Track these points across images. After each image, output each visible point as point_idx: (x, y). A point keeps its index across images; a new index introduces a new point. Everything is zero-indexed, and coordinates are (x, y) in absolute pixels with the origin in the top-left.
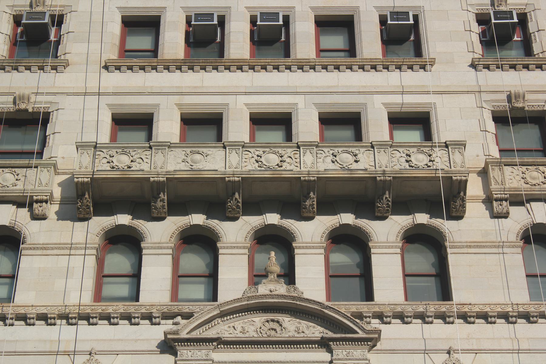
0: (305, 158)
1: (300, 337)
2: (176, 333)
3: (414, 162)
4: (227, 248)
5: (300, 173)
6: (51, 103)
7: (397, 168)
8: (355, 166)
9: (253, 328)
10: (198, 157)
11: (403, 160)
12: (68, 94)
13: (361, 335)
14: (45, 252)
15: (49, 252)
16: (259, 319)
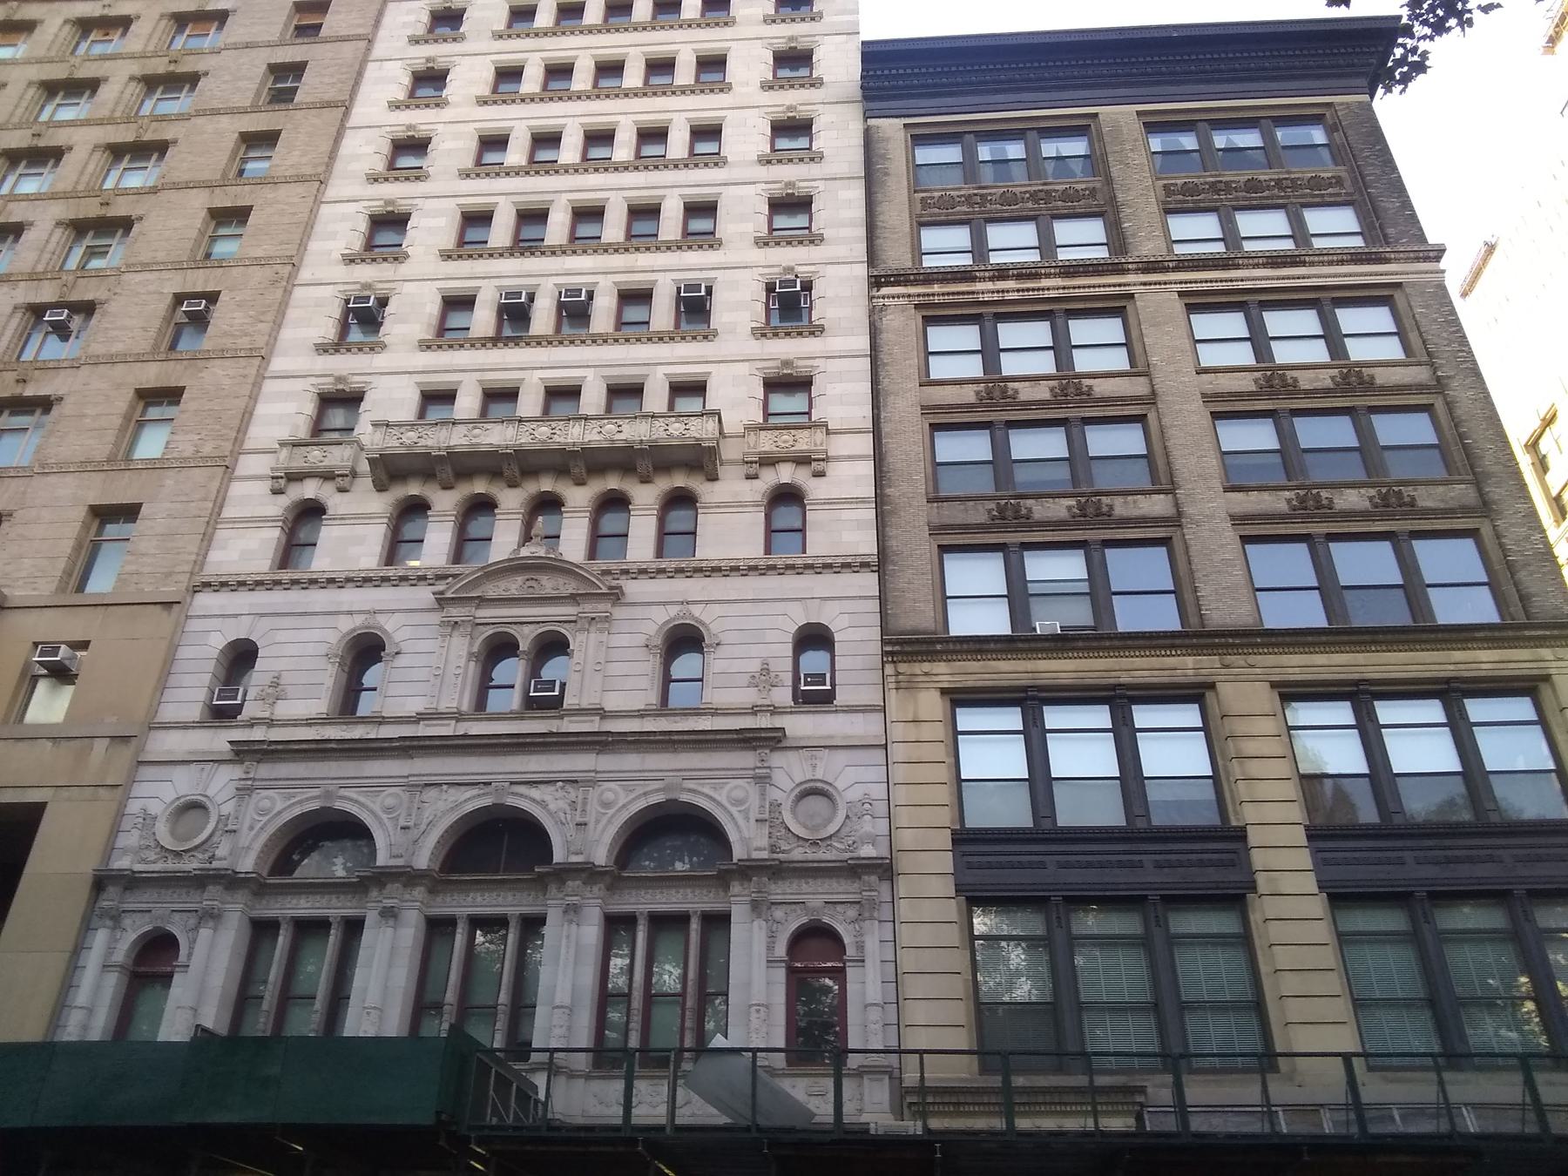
0: (574, 430)
1: (555, 593)
2: (442, 593)
3: (671, 431)
4: (504, 514)
5: (567, 444)
7: (654, 437)
8: (618, 437)
9: (514, 586)
10: (477, 431)
11: (662, 429)
12: (382, 374)
13: (605, 590)
14: (343, 522)
15: (347, 522)
16: (520, 579)
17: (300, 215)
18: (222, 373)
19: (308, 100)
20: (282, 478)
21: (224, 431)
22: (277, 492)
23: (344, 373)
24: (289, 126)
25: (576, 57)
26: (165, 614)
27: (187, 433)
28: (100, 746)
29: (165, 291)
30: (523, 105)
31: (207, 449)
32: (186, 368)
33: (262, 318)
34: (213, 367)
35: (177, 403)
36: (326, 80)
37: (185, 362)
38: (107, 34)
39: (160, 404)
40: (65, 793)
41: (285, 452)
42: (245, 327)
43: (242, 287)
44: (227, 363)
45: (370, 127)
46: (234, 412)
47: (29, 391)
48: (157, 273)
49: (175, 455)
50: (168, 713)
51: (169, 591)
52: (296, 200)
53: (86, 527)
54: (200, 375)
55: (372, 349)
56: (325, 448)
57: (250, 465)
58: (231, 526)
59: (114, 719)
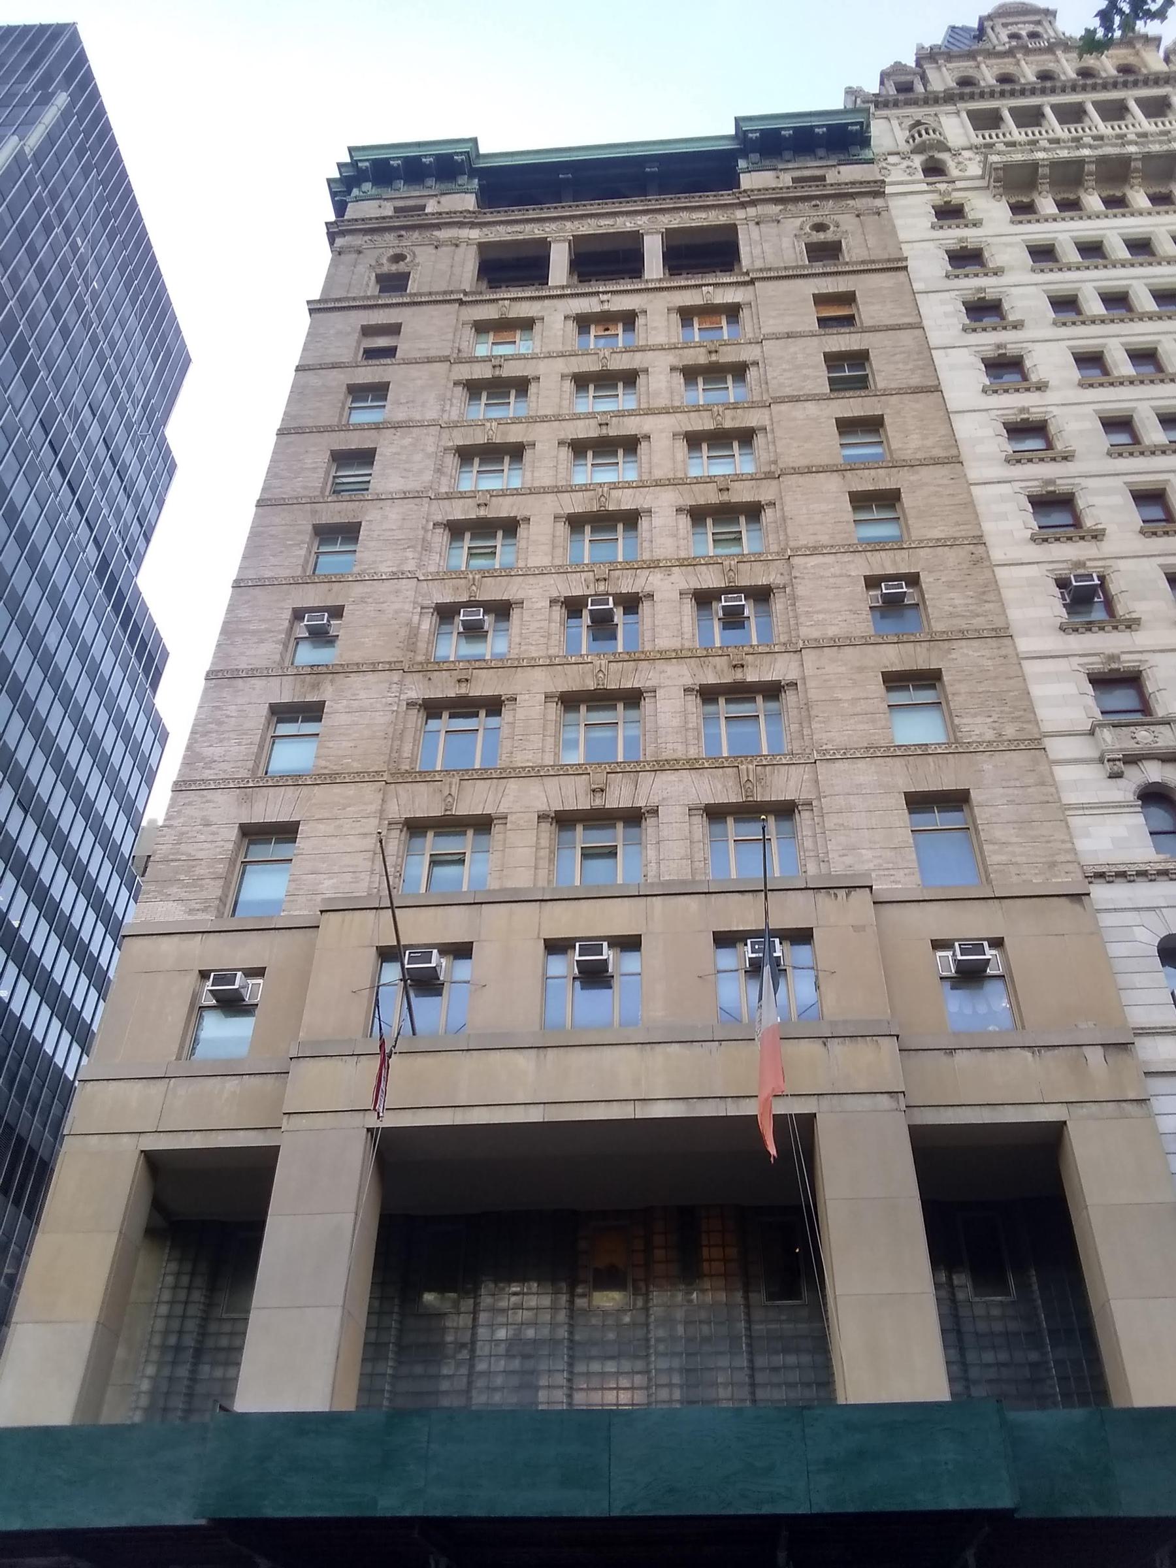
6: (1140, 661)
12: (1154, 651)
17: (961, 497)
18: (976, 654)
19: (893, 386)
20: (1119, 760)
21: (1017, 714)
22: (1116, 776)
23: (1116, 651)
24: (888, 411)
25: (1159, 341)
26: (1077, 907)
27: (975, 716)
28: (1095, 1056)
29: (853, 574)
30: (1132, 387)
31: (1010, 731)
32: (928, 650)
33: (985, 598)
34: (961, 648)
35: (319, 719)
36: (901, 366)
37: (922, 644)
38: (607, 329)
39: (906, 688)
40: (1084, 1110)
41: (1107, 735)
42: (971, 608)
43: (941, 568)
44: (976, 643)
45: (975, 411)
46: (1016, 693)
47: (751, 677)
48: (832, 556)
49: (974, 738)
50: (1139, 1017)
51: (1068, 881)
52: (946, 481)
53: (238, 846)
54: (950, 656)
55: (1129, 627)
56: (1152, 728)
57: (1058, 748)
58: (1081, 812)
59: (1091, 1024)
